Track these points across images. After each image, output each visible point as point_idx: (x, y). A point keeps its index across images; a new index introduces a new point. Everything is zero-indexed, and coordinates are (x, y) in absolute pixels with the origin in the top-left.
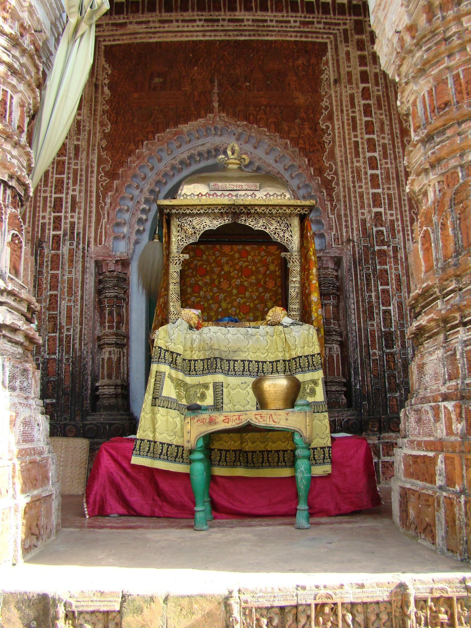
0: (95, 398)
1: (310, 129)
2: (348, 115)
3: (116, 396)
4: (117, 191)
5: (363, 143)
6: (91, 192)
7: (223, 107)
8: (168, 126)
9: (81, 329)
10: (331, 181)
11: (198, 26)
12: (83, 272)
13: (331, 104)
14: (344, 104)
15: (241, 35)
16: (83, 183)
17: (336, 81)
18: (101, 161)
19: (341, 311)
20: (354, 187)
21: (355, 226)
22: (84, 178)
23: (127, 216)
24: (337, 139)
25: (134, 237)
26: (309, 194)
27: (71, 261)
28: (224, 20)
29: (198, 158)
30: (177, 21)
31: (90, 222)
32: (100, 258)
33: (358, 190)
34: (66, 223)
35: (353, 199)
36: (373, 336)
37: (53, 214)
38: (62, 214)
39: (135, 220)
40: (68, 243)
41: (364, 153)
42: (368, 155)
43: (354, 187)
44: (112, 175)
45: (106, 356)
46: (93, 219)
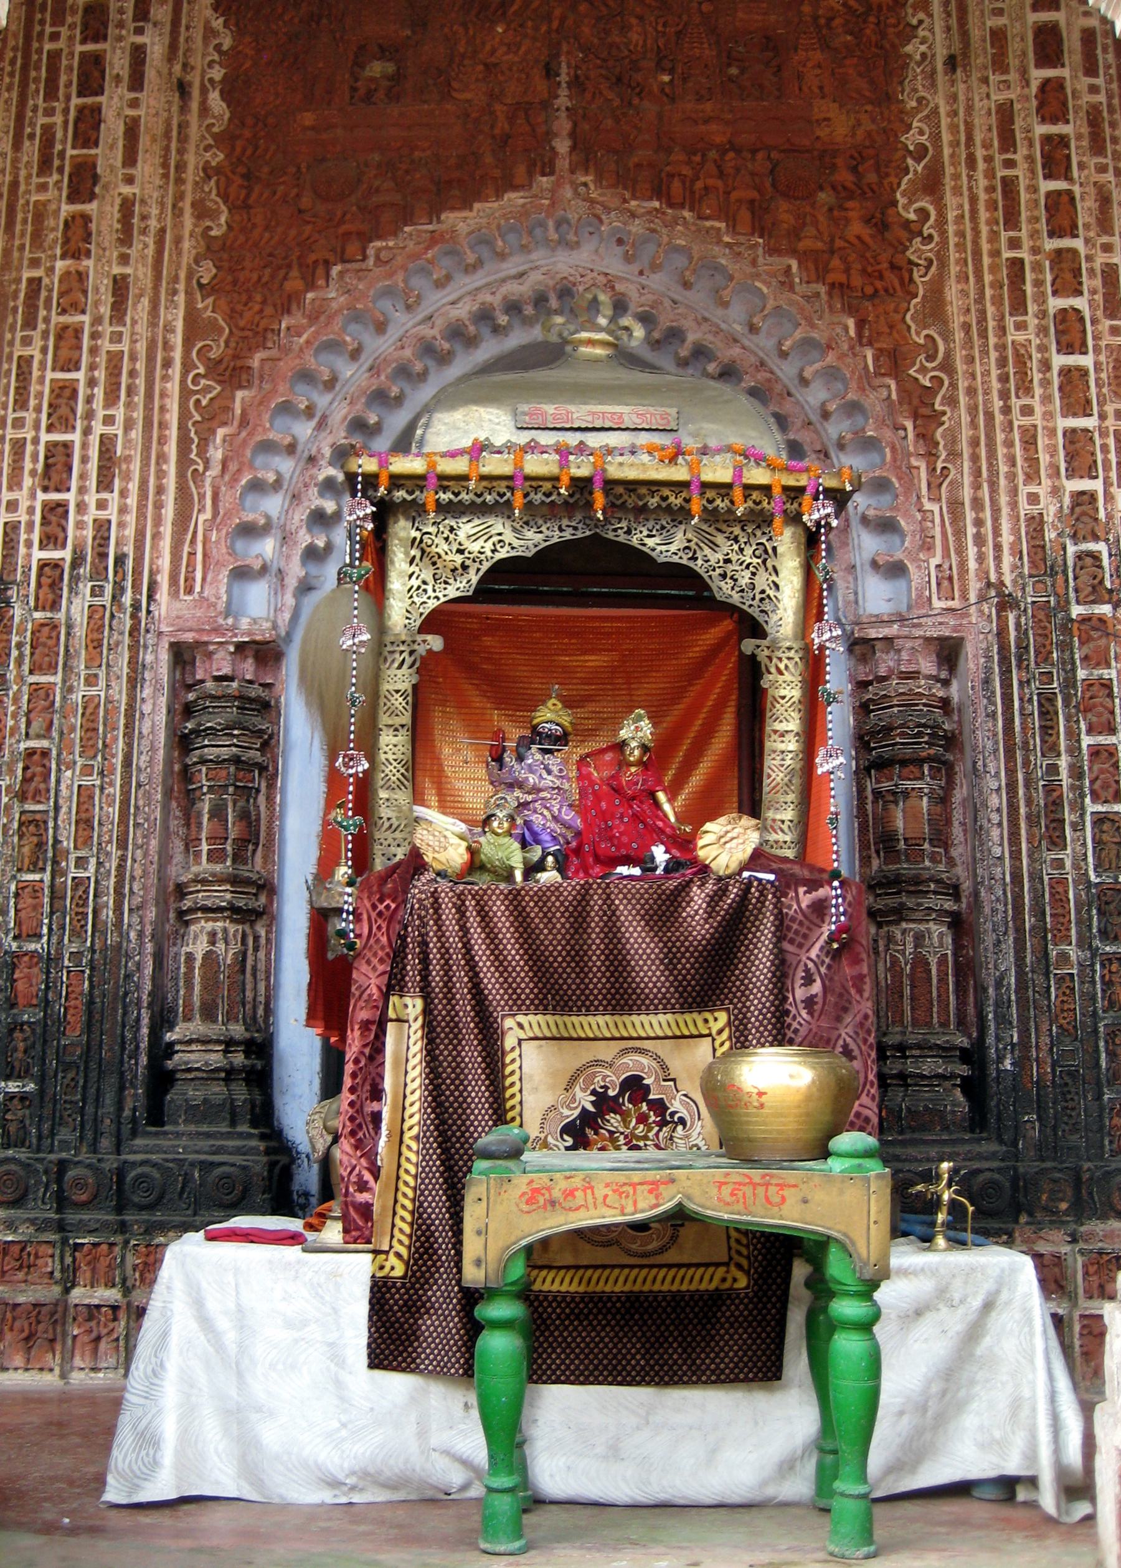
0: (161, 1079)
1: (867, 220)
2: (990, 174)
3: (230, 1074)
4: (244, 422)
5: (1037, 267)
6: (163, 425)
7: (585, 153)
8: (407, 216)
9: (123, 859)
10: (931, 392)
12: (134, 682)
13: (936, 138)
14: (978, 138)
16: (139, 399)
17: (951, 63)
18: (194, 328)
19: (957, 816)
20: (1006, 410)
21: (1006, 539)
22: (140, 382)
23: (273, 505)
24: (953, 255)
25: (296, 570)
26: (858, 433)
29: (503, 320)
31: (158, 521)
32: (189, 637)
33: (1019, 421)
34: (80, 525)
35: (1001, 451)
36: (1060, 900)
37: (41, 496)
38: (71, 497)
39: (300, 515)
40: (86, 588)
41: (1041, 298)
42: (1055, 304)
43: (1006, 410)
44: (231, 373)
45: (199, 948)
46: (169, 512)
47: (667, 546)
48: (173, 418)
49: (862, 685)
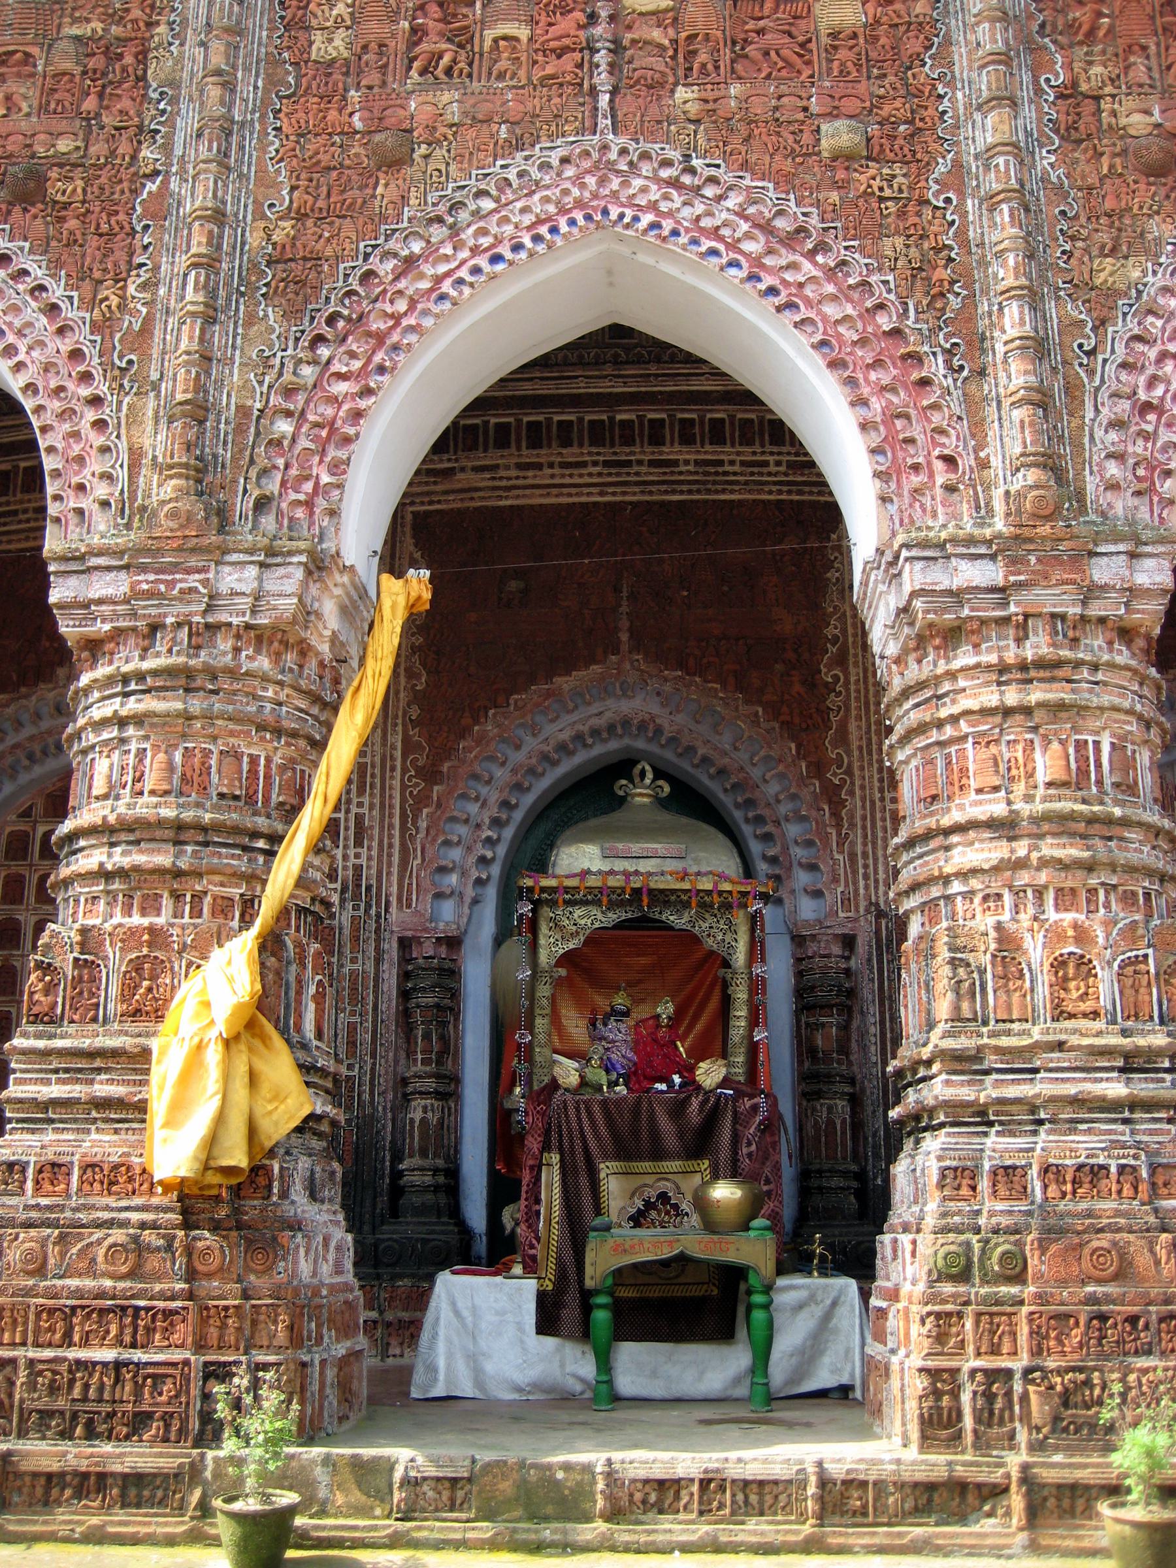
0: (397, 1191)
3: (436, 1188)
4: (439, 805)
6: (391, 807)
7: (638, 642)
8: (533, 681)
11: (590, 475)
12: (378, 960)
13: (844, 631)
15: (674, 492)
16: (377, 791)
18: (408, 747)
19: (854, 1036)
20: (882, 799)
22: (378, 781)
23: (456, 854)
24: (853, 704)
25: (470, 892)
26: (796, 812)
27: (355, 939)
28: (640, 462)
29: (590, 741)
30: (551, 465)
31: (390, 865)
32: (409, 934)
34: (345, 868)
35: (879, 824)
39: (472, 859)
40: (349, 905)
44: (431, 775)
45: (417, 1115)
46: (396, 859)
47: (678, 920)
48: (397, 802)
49: (799, 960)
